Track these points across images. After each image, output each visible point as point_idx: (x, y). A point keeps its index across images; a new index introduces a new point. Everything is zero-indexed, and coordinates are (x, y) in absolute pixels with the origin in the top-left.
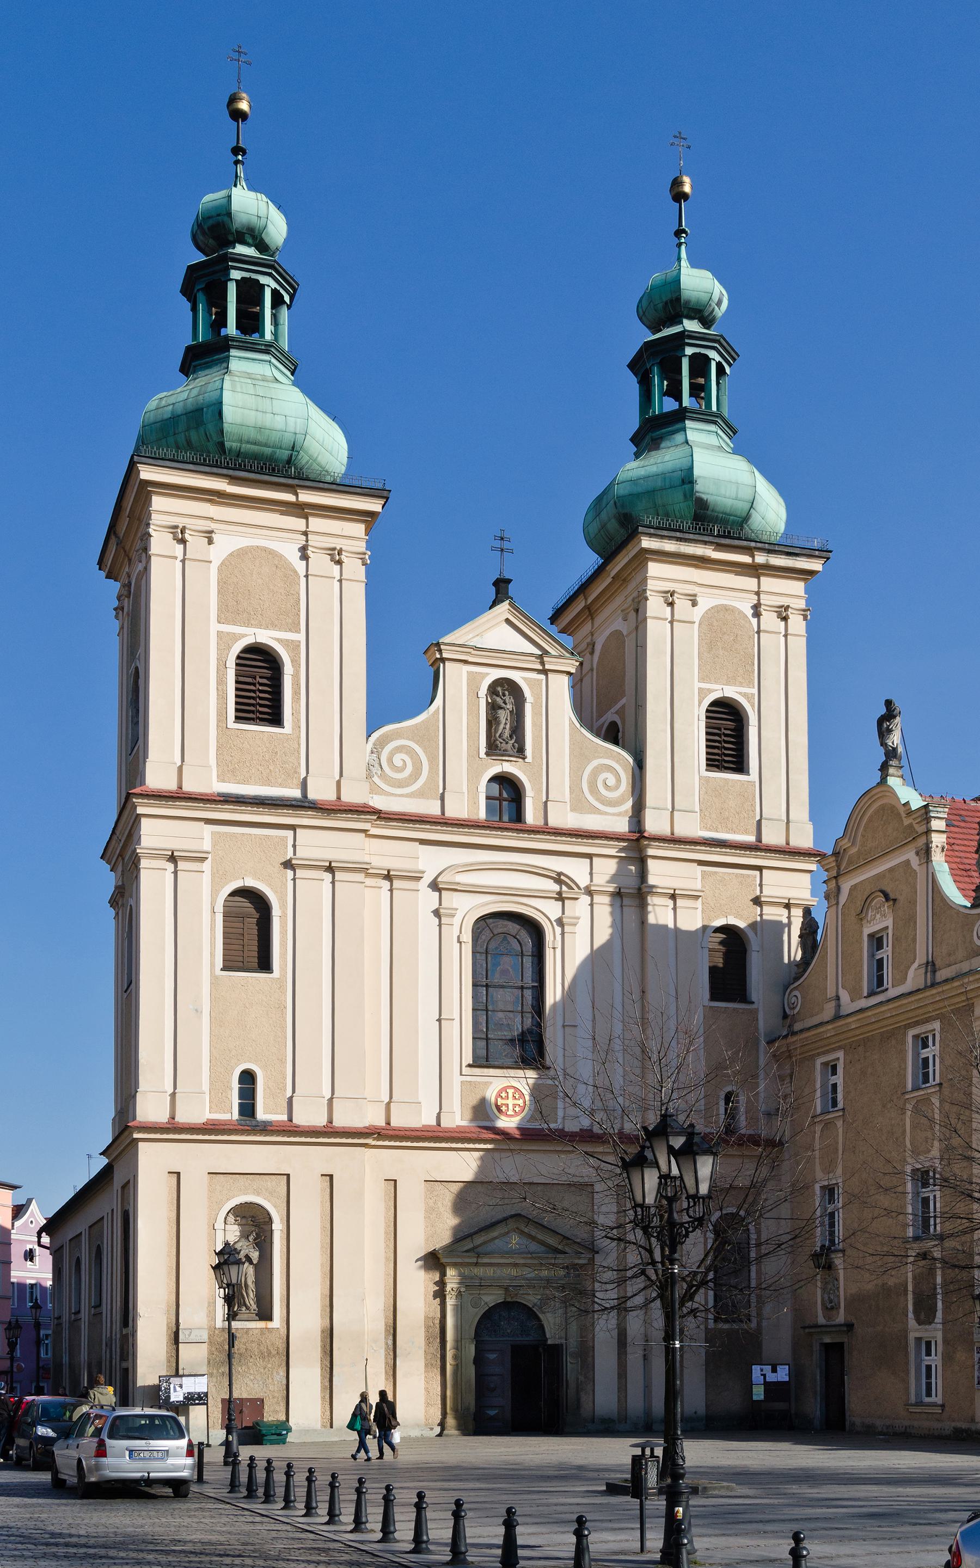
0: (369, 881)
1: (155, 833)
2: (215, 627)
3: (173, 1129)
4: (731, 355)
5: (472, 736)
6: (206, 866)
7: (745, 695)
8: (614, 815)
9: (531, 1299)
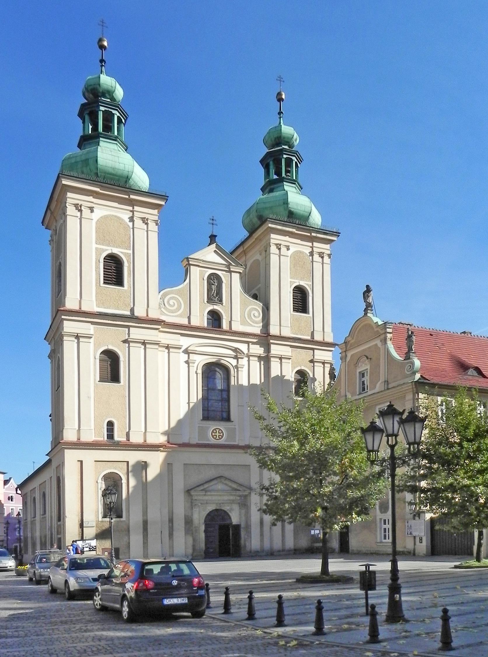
0: (160, 349)
1: (70, 326)
2: (94, 246)
3: (79, 445)
4: (300, 160)
5: (202, 295)
6: (92, 340)
7: (307, 285)
9: (226, 508)
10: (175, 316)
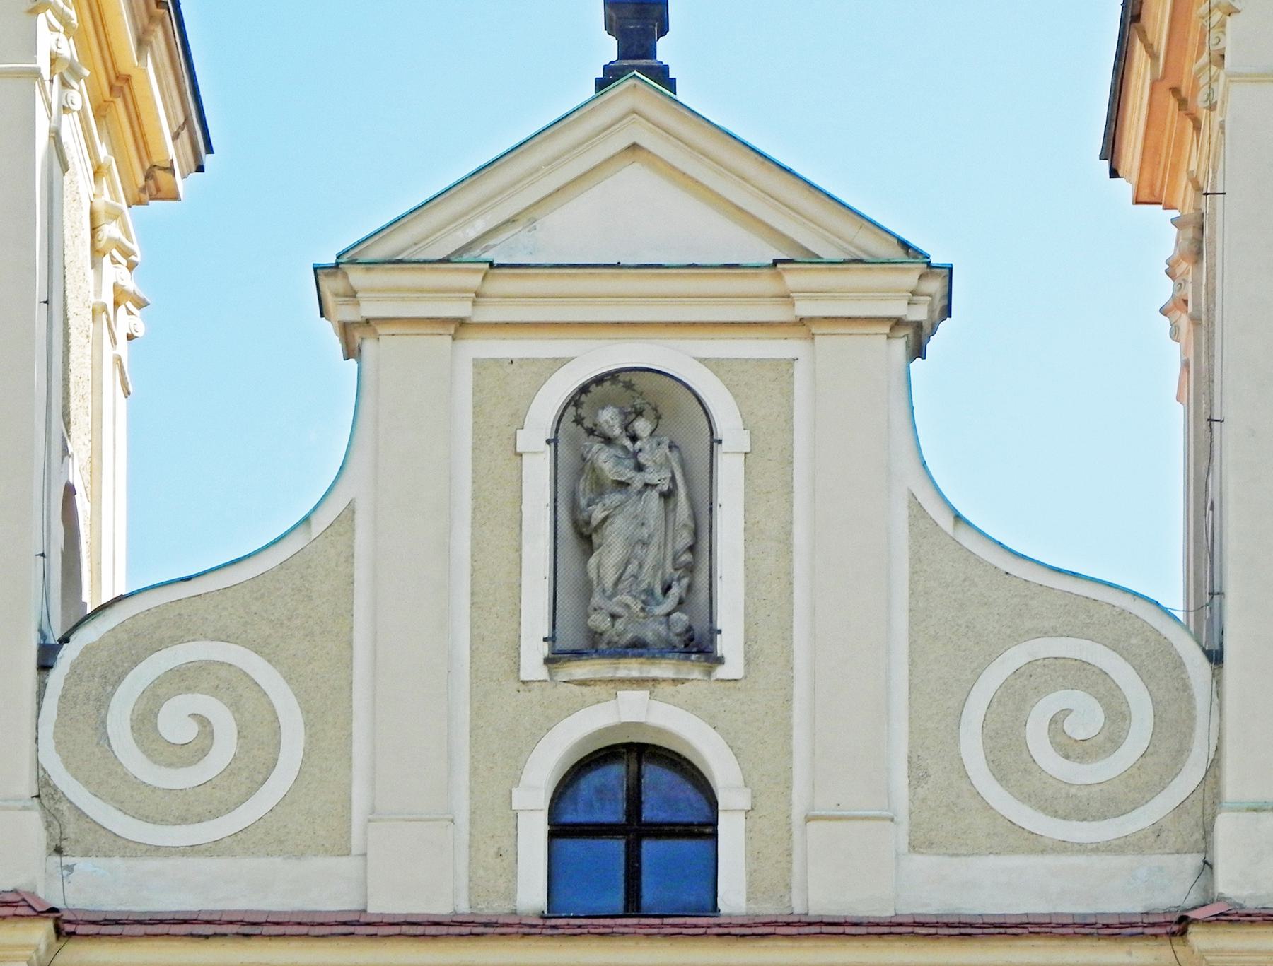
10: (214, 849)
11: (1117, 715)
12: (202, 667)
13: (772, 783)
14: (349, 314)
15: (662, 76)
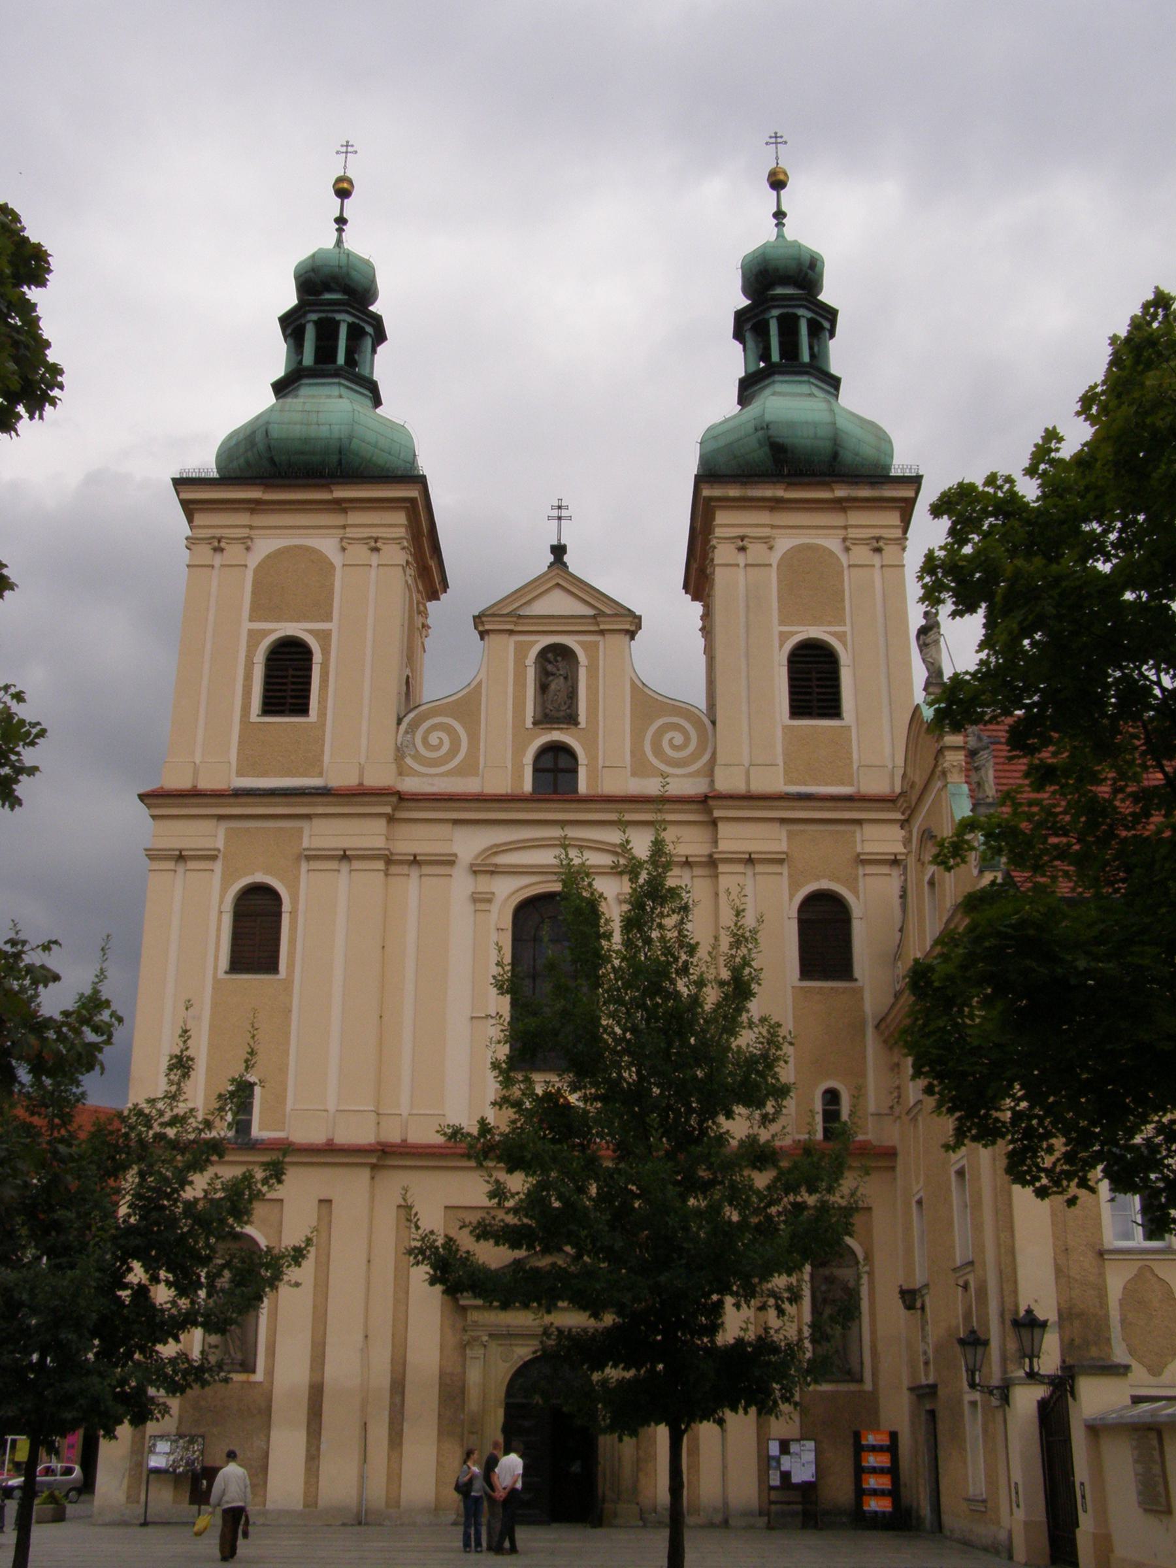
8: (684, 776)
11: (687, 739)
12: (441, 724)
13: (593, 758)
14: (481, 628)
15: (565, 565)
